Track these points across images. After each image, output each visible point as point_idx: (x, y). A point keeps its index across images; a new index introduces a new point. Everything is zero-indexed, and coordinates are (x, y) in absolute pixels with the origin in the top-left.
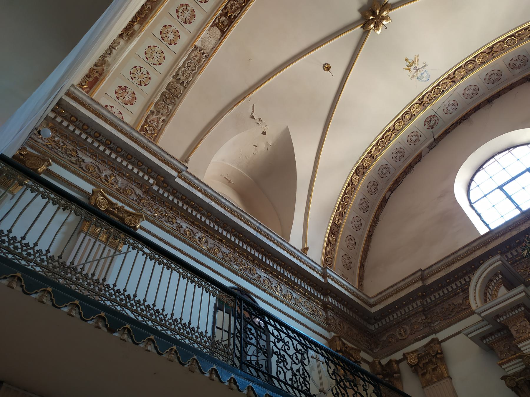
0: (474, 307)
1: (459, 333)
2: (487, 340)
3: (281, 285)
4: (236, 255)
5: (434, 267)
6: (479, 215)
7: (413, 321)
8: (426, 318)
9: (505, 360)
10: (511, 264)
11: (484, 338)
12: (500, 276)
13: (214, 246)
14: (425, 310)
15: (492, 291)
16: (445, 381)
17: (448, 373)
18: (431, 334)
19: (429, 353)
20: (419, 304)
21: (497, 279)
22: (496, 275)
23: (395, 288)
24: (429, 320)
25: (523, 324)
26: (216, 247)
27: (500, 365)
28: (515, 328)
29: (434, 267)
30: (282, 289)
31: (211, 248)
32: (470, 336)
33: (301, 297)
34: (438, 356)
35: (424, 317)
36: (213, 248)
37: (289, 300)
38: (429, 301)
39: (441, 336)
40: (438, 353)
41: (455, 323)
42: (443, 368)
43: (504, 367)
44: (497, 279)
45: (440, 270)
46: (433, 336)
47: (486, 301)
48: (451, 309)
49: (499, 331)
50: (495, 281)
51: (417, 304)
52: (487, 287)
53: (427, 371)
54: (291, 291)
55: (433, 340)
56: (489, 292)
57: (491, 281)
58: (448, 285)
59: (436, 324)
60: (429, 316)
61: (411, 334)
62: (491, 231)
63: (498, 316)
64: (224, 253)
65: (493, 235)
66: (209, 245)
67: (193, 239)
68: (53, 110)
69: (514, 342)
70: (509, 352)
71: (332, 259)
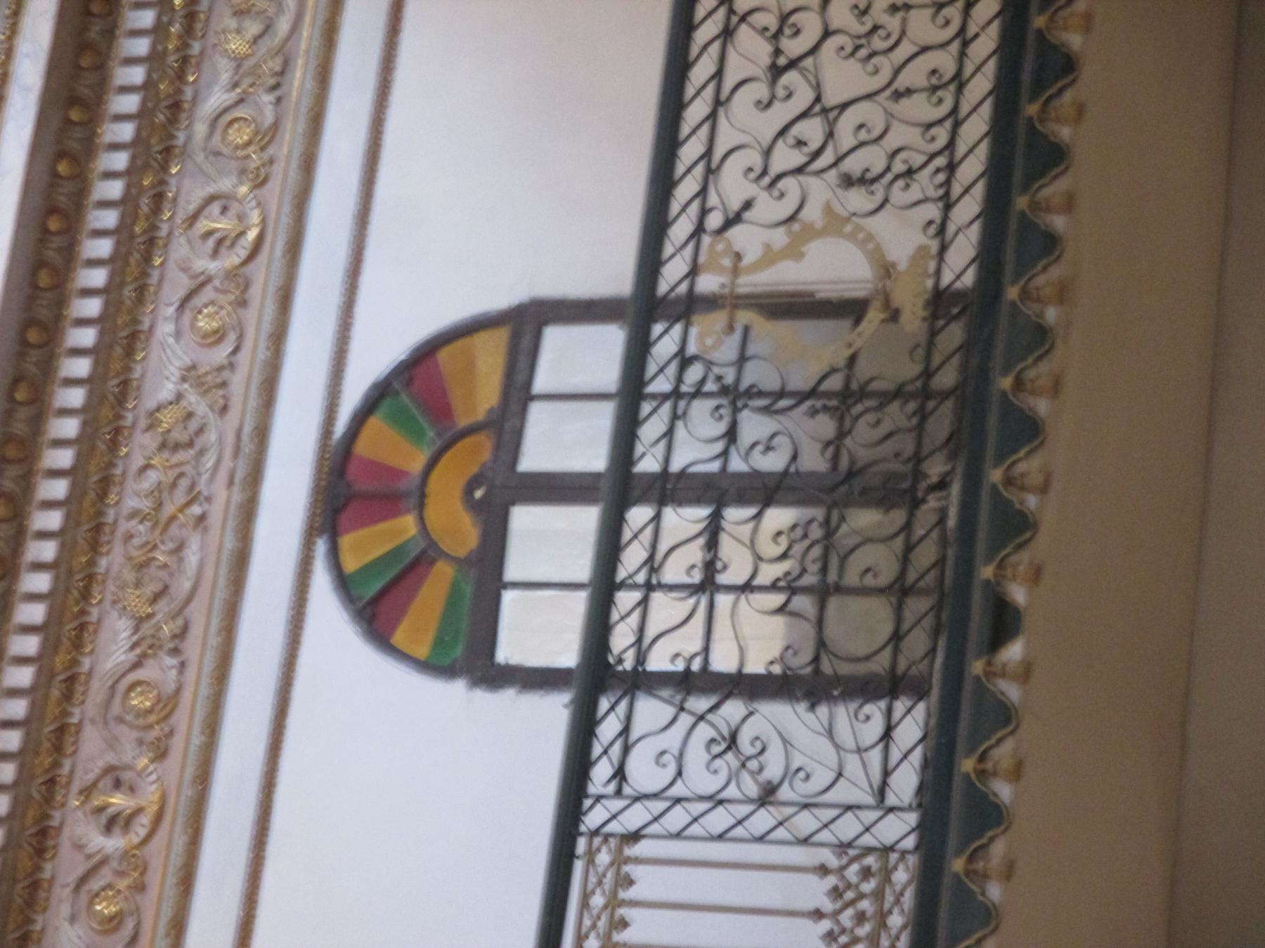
3: (189, 204)
4: (113, 561)
13: (120, 720)
26: (116, 708)
30: (212, 199)
31: (140, 742)
33: (212, 39)
36: (138, 728)
37: (267, 136)
54: (200, 129)
64: (133, 647)
66: (127, 757)
67: (134, 862)
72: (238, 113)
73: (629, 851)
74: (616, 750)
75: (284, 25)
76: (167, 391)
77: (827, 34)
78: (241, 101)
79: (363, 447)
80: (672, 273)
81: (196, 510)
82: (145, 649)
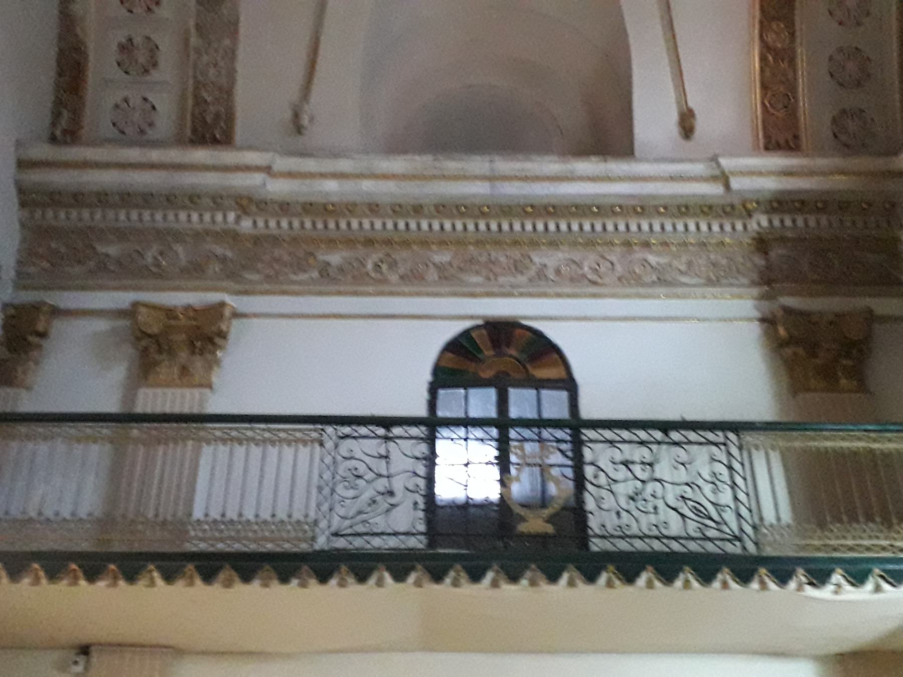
30: (612, 264)
68: (23, 204)
71: (793, 89)
72: (648, 267)
73: (317, 446)
74: (356, 434)
75: (684, 279)
76: (536, 259)
77: (643, 482)
78: (652, 267)
79: (518, 331)
80: (590, 434)
81: (492, 276)
82: (439, 267)
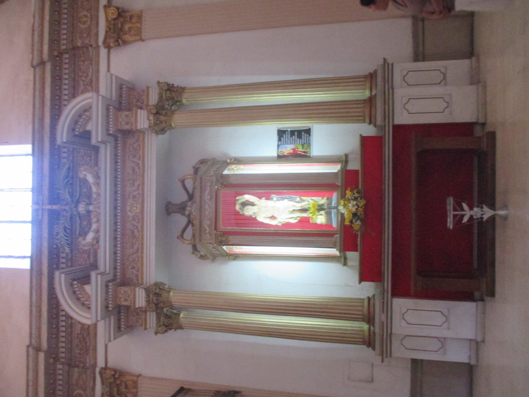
0: (88, 322)
1: (106, 346)
2: (122, 326)
5: (34, 331)
6: (10, 257)
7: (74, 381)
8: (78, 367)
9: (144, 323)
10: (72, 266)
11: (119, 328)
12: (75, 282)
14: (71, 364)
15: (83, 297)
16: (139, 382)
17: (134, 376)
18: (94, 370)
19: (110, 383)
20: (60, 366)
21: (76, 286)
22: (72, 285)
23: (31, 383)
24: (82, 365)
25: (122, 292)
27: (146, 329)
28: (122, 300)
29: (34, 331)
32: (112, 339)
34: (117, 376)
35: (76, 369)
38: (63, 355)
39: (101, 363)
40: (114, 375)
41: (96, 343)
42: (128, 377)
43: (148, 327)
44: (76, 286)
45: (39, 329)
46: (98, 370)
47: (89, 308)
48: (82, 339)
49: (119, 313)
50: (77, 289)
51: (60, 369)
52: (78, 299)
53: (124, 394)
55: (101, 374)
56: (84, 301)
57: (74, 292)
58: (58, 329)
59: (88, 361)
60: (77, 363)
61: (85, 390)
62: (31, 257)
63: (107, 307)
65: (36, 259)
69: (132, 308)
70: (140, 315)
